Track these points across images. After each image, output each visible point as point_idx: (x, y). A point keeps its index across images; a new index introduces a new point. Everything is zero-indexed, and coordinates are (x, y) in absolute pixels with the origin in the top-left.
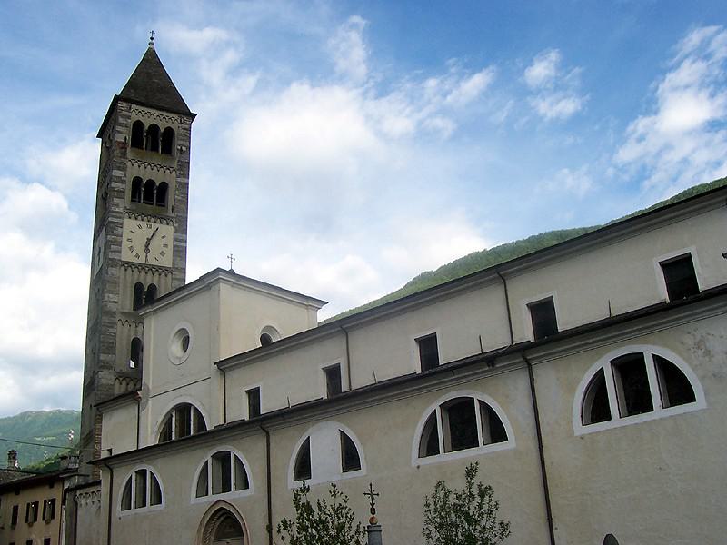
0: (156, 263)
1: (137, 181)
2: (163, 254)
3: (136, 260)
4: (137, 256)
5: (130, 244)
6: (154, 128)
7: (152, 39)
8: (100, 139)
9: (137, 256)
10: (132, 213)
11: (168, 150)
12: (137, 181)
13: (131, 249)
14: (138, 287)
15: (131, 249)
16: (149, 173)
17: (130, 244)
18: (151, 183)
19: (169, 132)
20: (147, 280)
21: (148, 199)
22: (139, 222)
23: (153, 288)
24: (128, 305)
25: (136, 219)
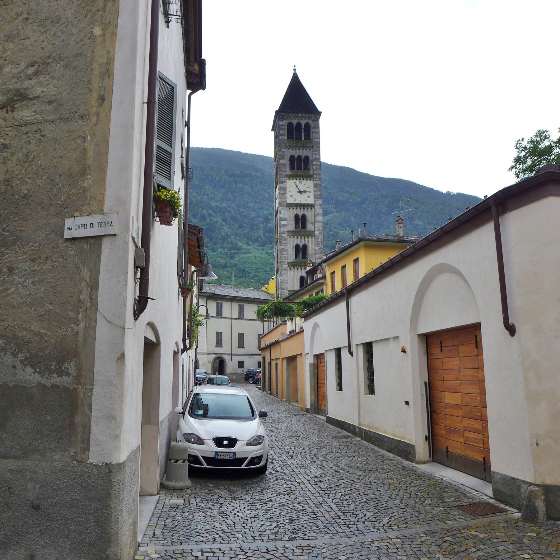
0: (306, 202)
1: (292, 158)
2: (309, 197)
3: (295, 202)
4: (295, 199)
5: (291, 194)
6: (299, 125)
7: (295, 66)
8: (273, 132)
9: (295, 199)
10: (290, 177)
11: (308, 136)
12: (292, 158)
13: (292, 196)
14: (297, 216)
15: (292, 196)
16: (297, 153)
17: (291, 194)
18: (299, 157)
19: (307, 125)
20: (300, 212)
21: (299, 168)
22: (295, 181)
23: (304, 216)
24: (291, 226)
25: (293, 179)
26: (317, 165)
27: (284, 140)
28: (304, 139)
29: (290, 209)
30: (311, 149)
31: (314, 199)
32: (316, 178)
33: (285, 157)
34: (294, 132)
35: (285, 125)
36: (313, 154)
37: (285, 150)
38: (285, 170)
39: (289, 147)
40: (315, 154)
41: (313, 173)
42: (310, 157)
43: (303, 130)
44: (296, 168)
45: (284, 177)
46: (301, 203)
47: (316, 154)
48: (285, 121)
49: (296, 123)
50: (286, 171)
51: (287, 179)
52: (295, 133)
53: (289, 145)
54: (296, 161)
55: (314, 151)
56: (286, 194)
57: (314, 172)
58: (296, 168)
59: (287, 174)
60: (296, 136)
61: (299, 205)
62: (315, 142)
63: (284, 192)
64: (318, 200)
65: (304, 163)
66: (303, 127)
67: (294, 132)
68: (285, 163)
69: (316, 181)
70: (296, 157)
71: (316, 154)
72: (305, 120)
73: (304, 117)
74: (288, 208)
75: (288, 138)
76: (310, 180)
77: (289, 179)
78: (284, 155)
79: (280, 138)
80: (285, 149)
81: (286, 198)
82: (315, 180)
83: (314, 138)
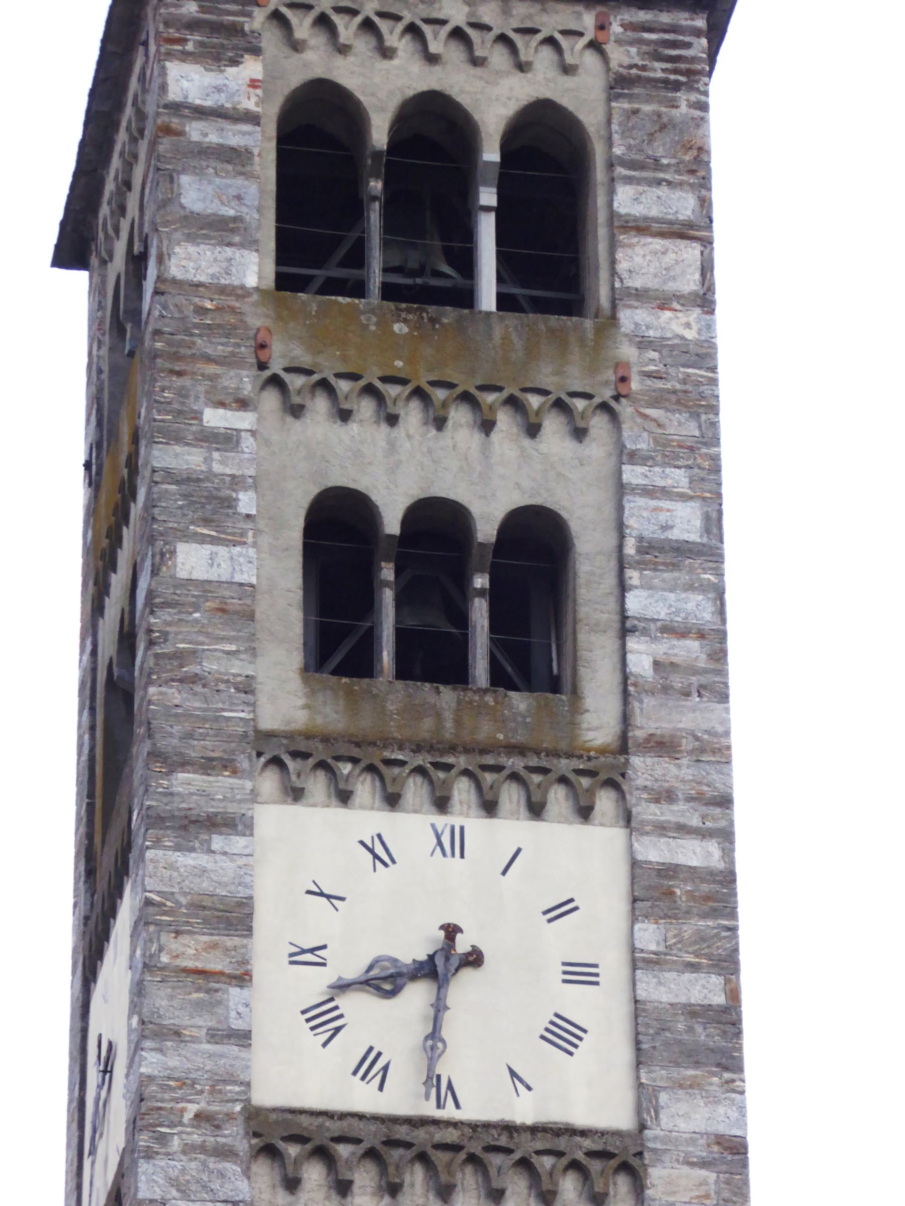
8: (82, 277)
26: (671, 630)
27: (241, 292)
28: (505, 302)
29: (292, 1184)
30: (599, 424)
31: (641, 1058)
32: (665, 796)
33: (246, 502)
34: (374, 216)
35: (253, 119)
36: (621, 489)
37: (243, 420)
38: (238, 668)
39: (296, 382)
40: (649, 492)
41: (626, 719)
42: (574, 526)
43: (488, 197)
44: (387, 657)
45: (227, 765)
46: (449, 1112)
47: (665, 493)
48: (252, 68)
49: (392, 106)
50: (247, 687)
51: (269, 782)
52: (386, 245)
53: (306, 360)
54: (388, 572)
55: (634, 457)
56: (243, 979)
57: (638, 719)
58: (387, 657)
59: (267, 723)
60: (386, 270)
61: (420, 1135)
62: (644, 344)
63: (216, 963)
64: (693, 1085)
65: (495, 595)
66: (491, 154)
67: (374, 216)
68: (248, 576)
69: (662, 829)
70: (392, 524)
71: (665, 493)
72: (522, 67)
73: (503, 39)
74: (263, 1170)
75: (284, 282)
76: (585, 813)
77: (296, 794)
78: (236, 482)
79: (175, 269)
80: (243, 404)
81: (243, 1038)
82: (646, 811)
83: (641, 296)
